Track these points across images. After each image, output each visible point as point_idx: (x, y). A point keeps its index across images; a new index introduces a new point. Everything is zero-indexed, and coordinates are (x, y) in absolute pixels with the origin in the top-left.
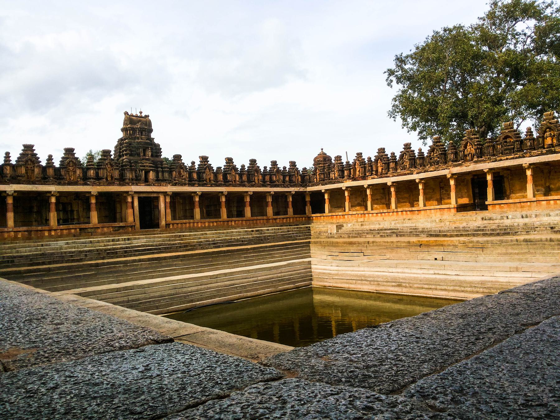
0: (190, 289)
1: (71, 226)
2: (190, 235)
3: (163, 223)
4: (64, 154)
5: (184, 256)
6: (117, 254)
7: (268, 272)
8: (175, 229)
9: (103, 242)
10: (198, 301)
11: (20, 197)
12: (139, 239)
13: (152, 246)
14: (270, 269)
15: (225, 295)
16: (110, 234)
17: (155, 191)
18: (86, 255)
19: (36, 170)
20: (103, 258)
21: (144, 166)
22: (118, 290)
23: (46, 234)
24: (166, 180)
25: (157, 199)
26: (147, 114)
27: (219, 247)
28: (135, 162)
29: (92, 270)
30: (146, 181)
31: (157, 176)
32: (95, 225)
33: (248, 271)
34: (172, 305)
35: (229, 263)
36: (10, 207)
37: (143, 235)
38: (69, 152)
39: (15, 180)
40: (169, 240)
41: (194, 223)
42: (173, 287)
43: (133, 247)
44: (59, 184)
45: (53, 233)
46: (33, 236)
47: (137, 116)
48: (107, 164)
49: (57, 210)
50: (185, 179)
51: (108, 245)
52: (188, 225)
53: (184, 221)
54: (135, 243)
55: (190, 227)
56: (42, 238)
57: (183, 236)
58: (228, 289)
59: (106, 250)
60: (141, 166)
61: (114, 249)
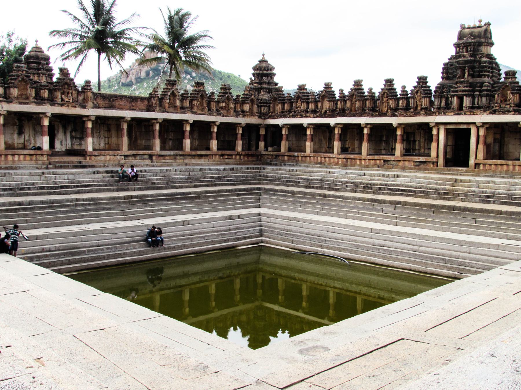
0: (335, 235)
1: (376, 157)
2: (470, 181)
3: (472, 162)
4: (385, 85)
5: (406, 204)
6: (372, 189)
7: (459, 248)
8: (486, 171)
9: (374, 176)
10: (327, 248)
11: (346, 127)
12: (408, 177)
13: (411, 187)
14: (460, 243)
15: (355, 252)
16: (410, 168)
17: (460, 121)
18: (347, 186)
19: (357, 103)
20: (355, 191)
21: (456, 91)
22: (289, 219)
23: (358, 162)
24: (481, 107)
25: (469, 130)
26: (487, 22)
27: (488, 202)
28: (450, 86)
29: (315, 199)
30: (460, 109)
31: (473, 103)
32: (397, 158)
33: (424, 237)
34: (303, 243)
35: (442, 224)
36: (337, 136)
37: (441, 174)
38: (389, 82)
39: (343, 113)
40: (437, 184)
41: (514, 166)
42: (325, 229)
43: (392, 185)
44: (372, 116)
45: (363, 162)
46: (349, 163)
47: (474, 28)
48: (417, 92)
49: (403, 141)
50: (510, 103)
51: (374, 180)
52: (505, 168)
53: (499, 162)
54: (399, 181)
55: (507, 171)
56: (353, 165)
57: (461, 181)
58: (368, 249)
59: (367, 184)
60: (453, 91)
61: (374, 184)
